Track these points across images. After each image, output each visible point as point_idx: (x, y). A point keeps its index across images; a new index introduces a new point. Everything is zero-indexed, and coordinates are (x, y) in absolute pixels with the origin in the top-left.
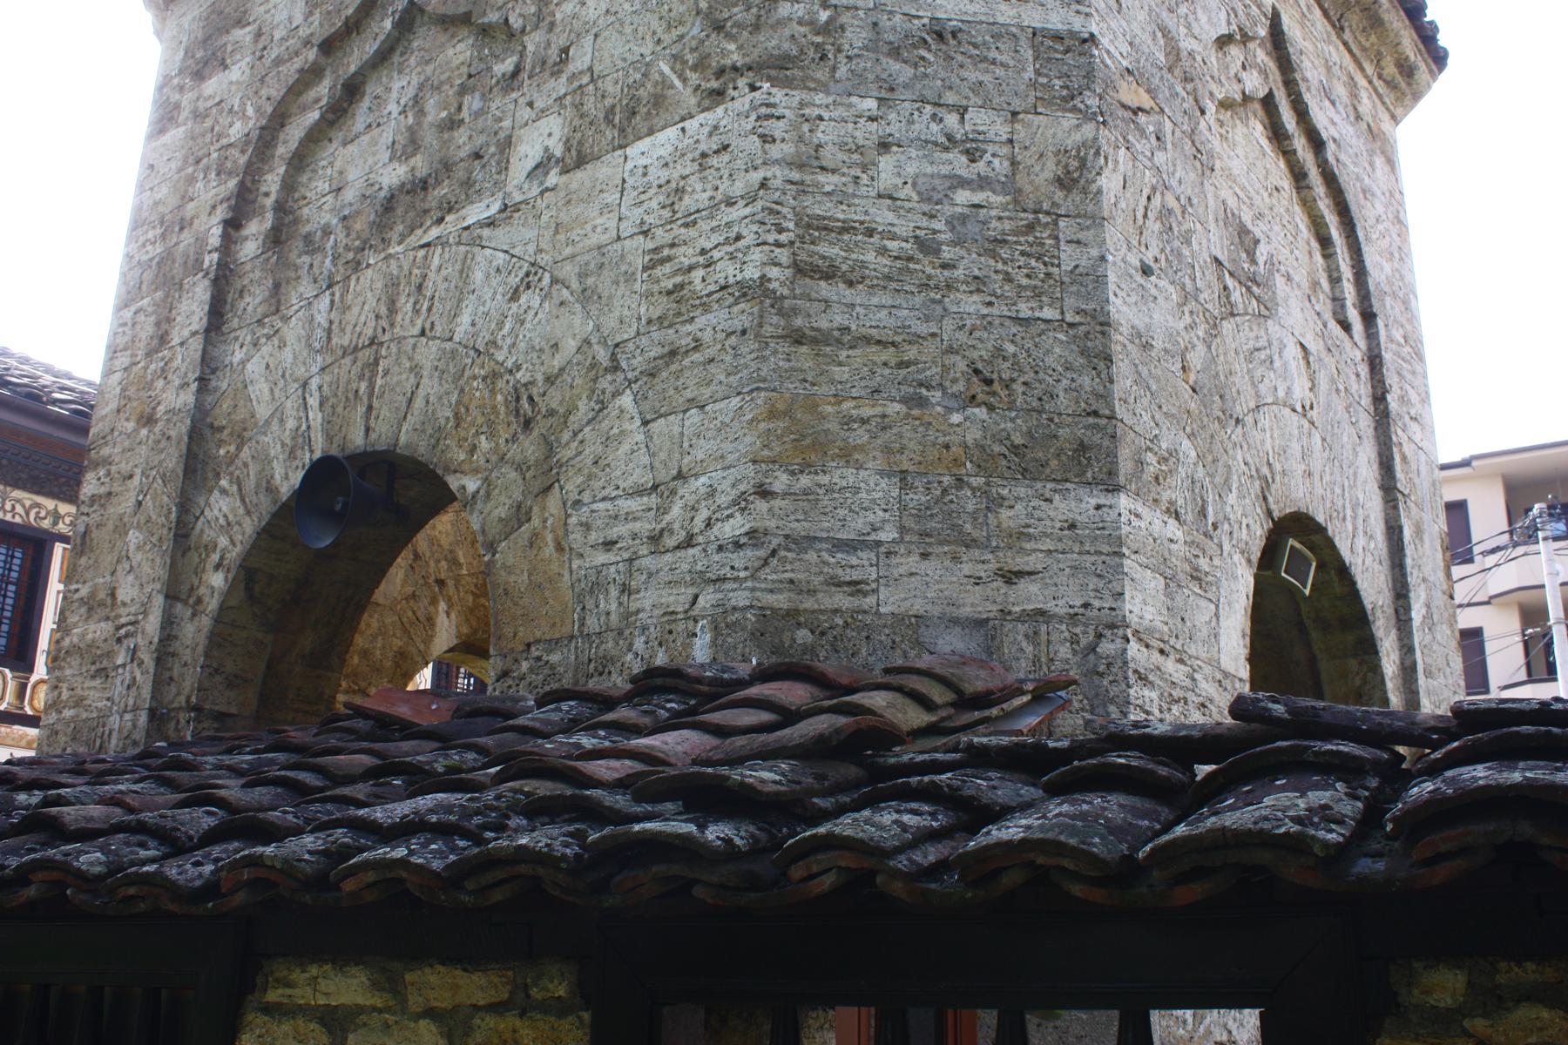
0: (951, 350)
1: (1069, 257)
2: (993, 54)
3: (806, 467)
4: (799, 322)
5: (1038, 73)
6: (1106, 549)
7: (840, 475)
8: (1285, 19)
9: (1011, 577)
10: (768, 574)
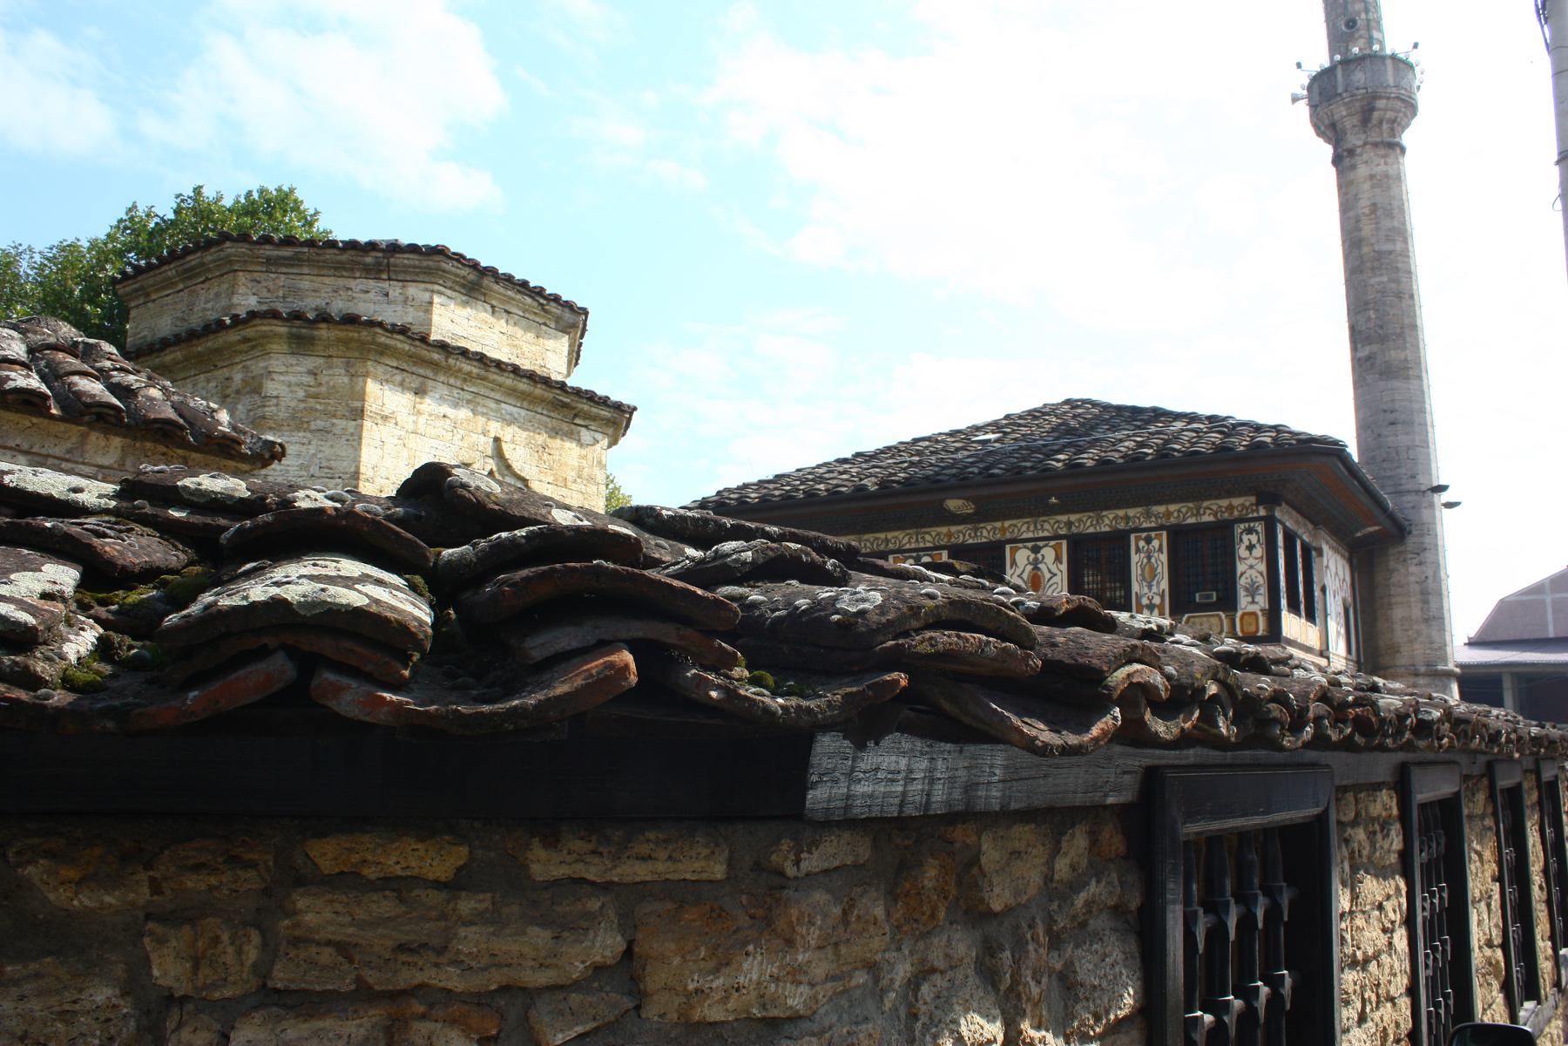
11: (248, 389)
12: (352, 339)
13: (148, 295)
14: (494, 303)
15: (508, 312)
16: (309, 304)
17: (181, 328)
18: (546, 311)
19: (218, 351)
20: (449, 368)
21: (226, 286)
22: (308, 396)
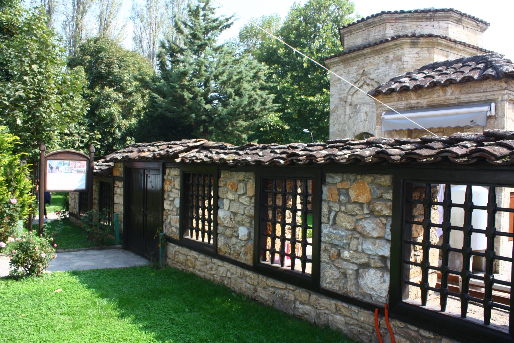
8: (366, 69)
12: (430, 42)
13: (351, 32)
14: (464, 25)
15: (467, 27)
16: (418, 31)
17: (366, 42)
18: (478, 26)
19: (384, 49)
20: (455, 48)
21: (382, 28)
22: (417, 61)
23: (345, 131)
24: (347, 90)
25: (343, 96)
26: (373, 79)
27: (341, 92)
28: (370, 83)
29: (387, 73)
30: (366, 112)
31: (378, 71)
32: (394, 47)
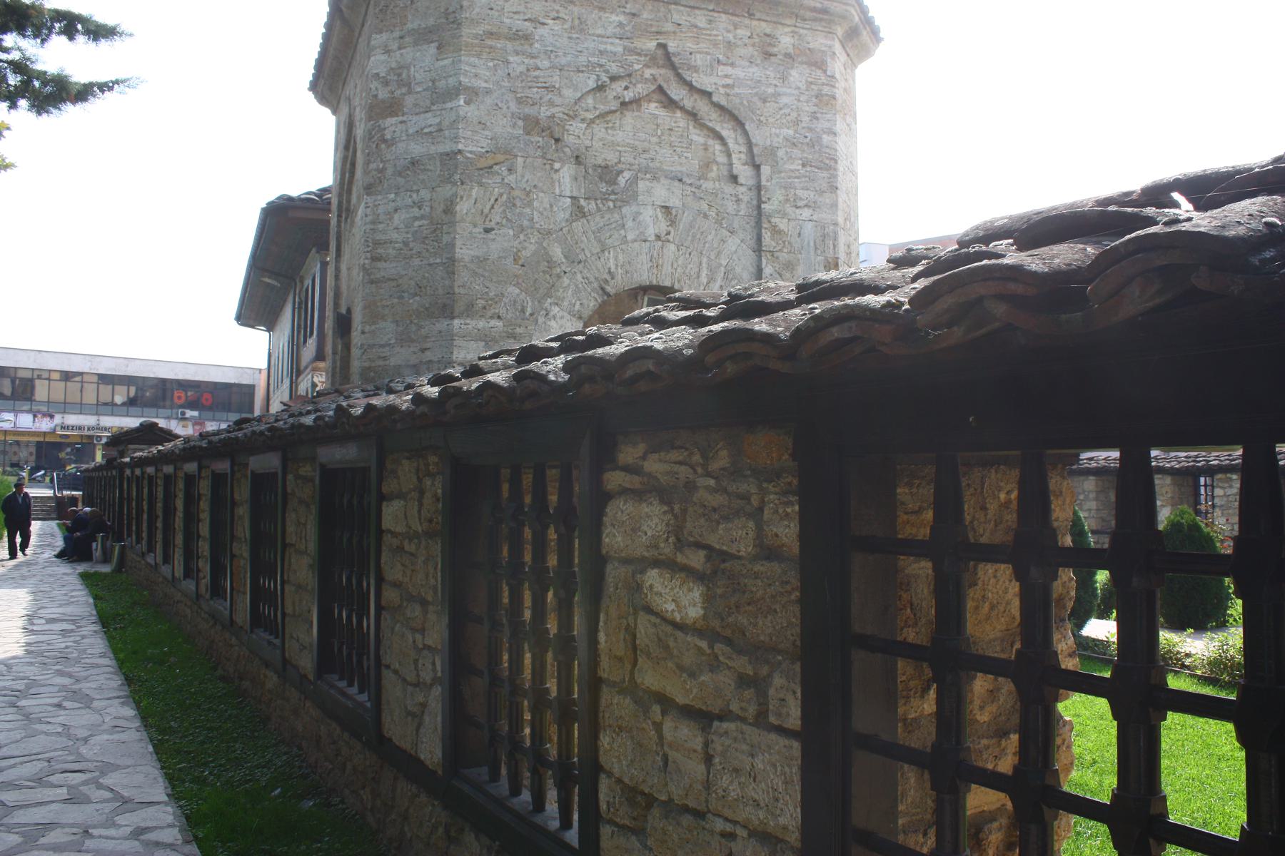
0: (411, 279)
1: (446, 239)
2: (428, 167)
3: (374, 323)
4: (372, 277)
5: (441, 171)
6: (449, 338)
7: (382, 324)
8: (672, 46)
9: (423, 350)
10: (364, 357)
11: (805, 59)
23: (551, 264)
24: (570, 94)
25: (544, 112)
26: (709, 95)
27: (534, 93)
28: (688, 104)
29: (771, 90)
30: (666, 209)
31: (729, 70)
32: (808, 14)
